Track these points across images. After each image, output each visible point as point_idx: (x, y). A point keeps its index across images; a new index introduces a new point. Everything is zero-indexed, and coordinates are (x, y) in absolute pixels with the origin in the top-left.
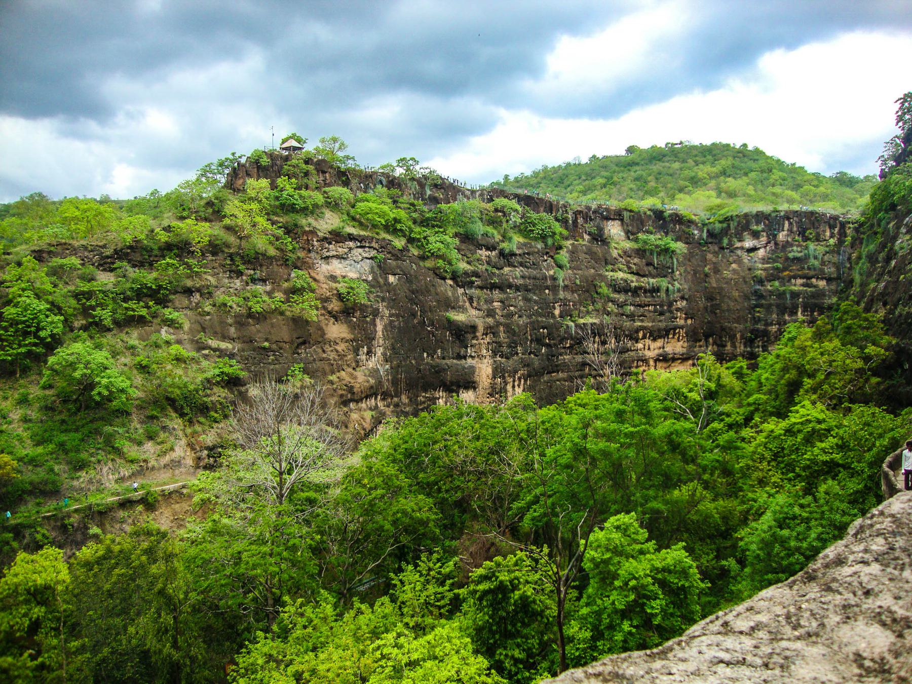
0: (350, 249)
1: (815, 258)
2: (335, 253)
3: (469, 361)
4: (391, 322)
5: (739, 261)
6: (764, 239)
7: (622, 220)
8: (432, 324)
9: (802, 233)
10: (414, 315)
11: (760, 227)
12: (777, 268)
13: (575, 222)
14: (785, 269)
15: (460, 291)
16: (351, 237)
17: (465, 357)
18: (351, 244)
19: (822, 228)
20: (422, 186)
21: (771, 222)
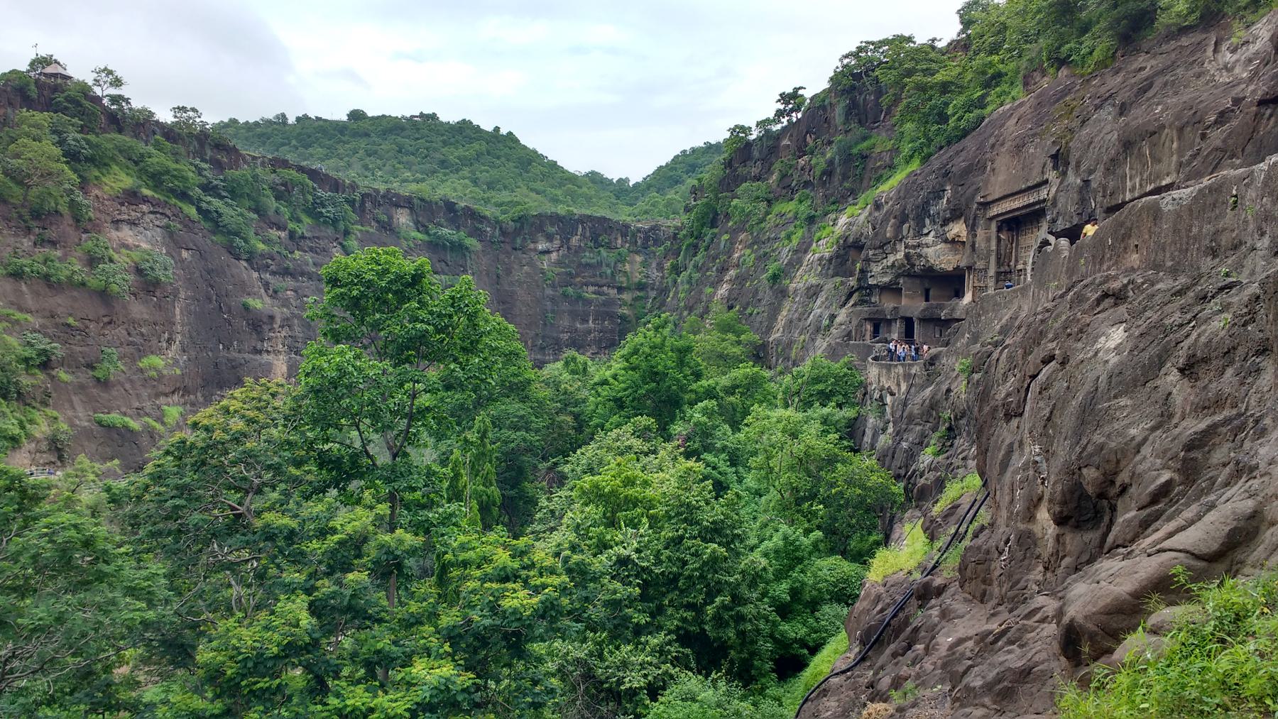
0: (144, 213)
1: (608, 265)
2: (126, 217)
3: (265, 356)
4: (188, 305)
5: (531, 263)
6: (557, 243)
7: (411, 209)
8: (230, 312)
9: (595, 238)
10: (210, 299)
11: (552, 230)
12: (570, 274)
13: (363, 203)
14: (578, 275)
15: (255, 275)
16: (146, 200)
17: (260, 352)
18: (145, 208)
19: (613, 236)
20: (202, 145)
21: (566, 225)
